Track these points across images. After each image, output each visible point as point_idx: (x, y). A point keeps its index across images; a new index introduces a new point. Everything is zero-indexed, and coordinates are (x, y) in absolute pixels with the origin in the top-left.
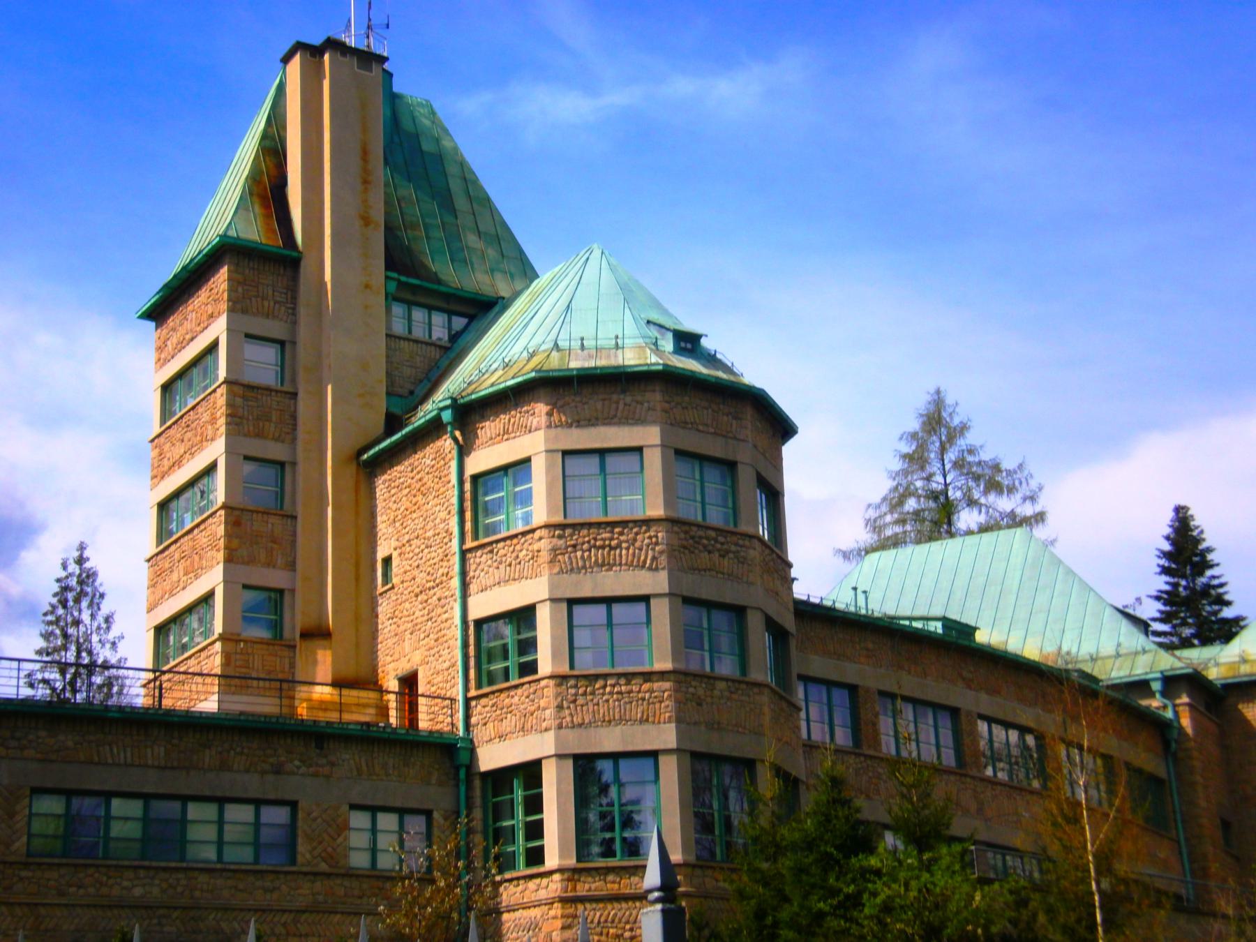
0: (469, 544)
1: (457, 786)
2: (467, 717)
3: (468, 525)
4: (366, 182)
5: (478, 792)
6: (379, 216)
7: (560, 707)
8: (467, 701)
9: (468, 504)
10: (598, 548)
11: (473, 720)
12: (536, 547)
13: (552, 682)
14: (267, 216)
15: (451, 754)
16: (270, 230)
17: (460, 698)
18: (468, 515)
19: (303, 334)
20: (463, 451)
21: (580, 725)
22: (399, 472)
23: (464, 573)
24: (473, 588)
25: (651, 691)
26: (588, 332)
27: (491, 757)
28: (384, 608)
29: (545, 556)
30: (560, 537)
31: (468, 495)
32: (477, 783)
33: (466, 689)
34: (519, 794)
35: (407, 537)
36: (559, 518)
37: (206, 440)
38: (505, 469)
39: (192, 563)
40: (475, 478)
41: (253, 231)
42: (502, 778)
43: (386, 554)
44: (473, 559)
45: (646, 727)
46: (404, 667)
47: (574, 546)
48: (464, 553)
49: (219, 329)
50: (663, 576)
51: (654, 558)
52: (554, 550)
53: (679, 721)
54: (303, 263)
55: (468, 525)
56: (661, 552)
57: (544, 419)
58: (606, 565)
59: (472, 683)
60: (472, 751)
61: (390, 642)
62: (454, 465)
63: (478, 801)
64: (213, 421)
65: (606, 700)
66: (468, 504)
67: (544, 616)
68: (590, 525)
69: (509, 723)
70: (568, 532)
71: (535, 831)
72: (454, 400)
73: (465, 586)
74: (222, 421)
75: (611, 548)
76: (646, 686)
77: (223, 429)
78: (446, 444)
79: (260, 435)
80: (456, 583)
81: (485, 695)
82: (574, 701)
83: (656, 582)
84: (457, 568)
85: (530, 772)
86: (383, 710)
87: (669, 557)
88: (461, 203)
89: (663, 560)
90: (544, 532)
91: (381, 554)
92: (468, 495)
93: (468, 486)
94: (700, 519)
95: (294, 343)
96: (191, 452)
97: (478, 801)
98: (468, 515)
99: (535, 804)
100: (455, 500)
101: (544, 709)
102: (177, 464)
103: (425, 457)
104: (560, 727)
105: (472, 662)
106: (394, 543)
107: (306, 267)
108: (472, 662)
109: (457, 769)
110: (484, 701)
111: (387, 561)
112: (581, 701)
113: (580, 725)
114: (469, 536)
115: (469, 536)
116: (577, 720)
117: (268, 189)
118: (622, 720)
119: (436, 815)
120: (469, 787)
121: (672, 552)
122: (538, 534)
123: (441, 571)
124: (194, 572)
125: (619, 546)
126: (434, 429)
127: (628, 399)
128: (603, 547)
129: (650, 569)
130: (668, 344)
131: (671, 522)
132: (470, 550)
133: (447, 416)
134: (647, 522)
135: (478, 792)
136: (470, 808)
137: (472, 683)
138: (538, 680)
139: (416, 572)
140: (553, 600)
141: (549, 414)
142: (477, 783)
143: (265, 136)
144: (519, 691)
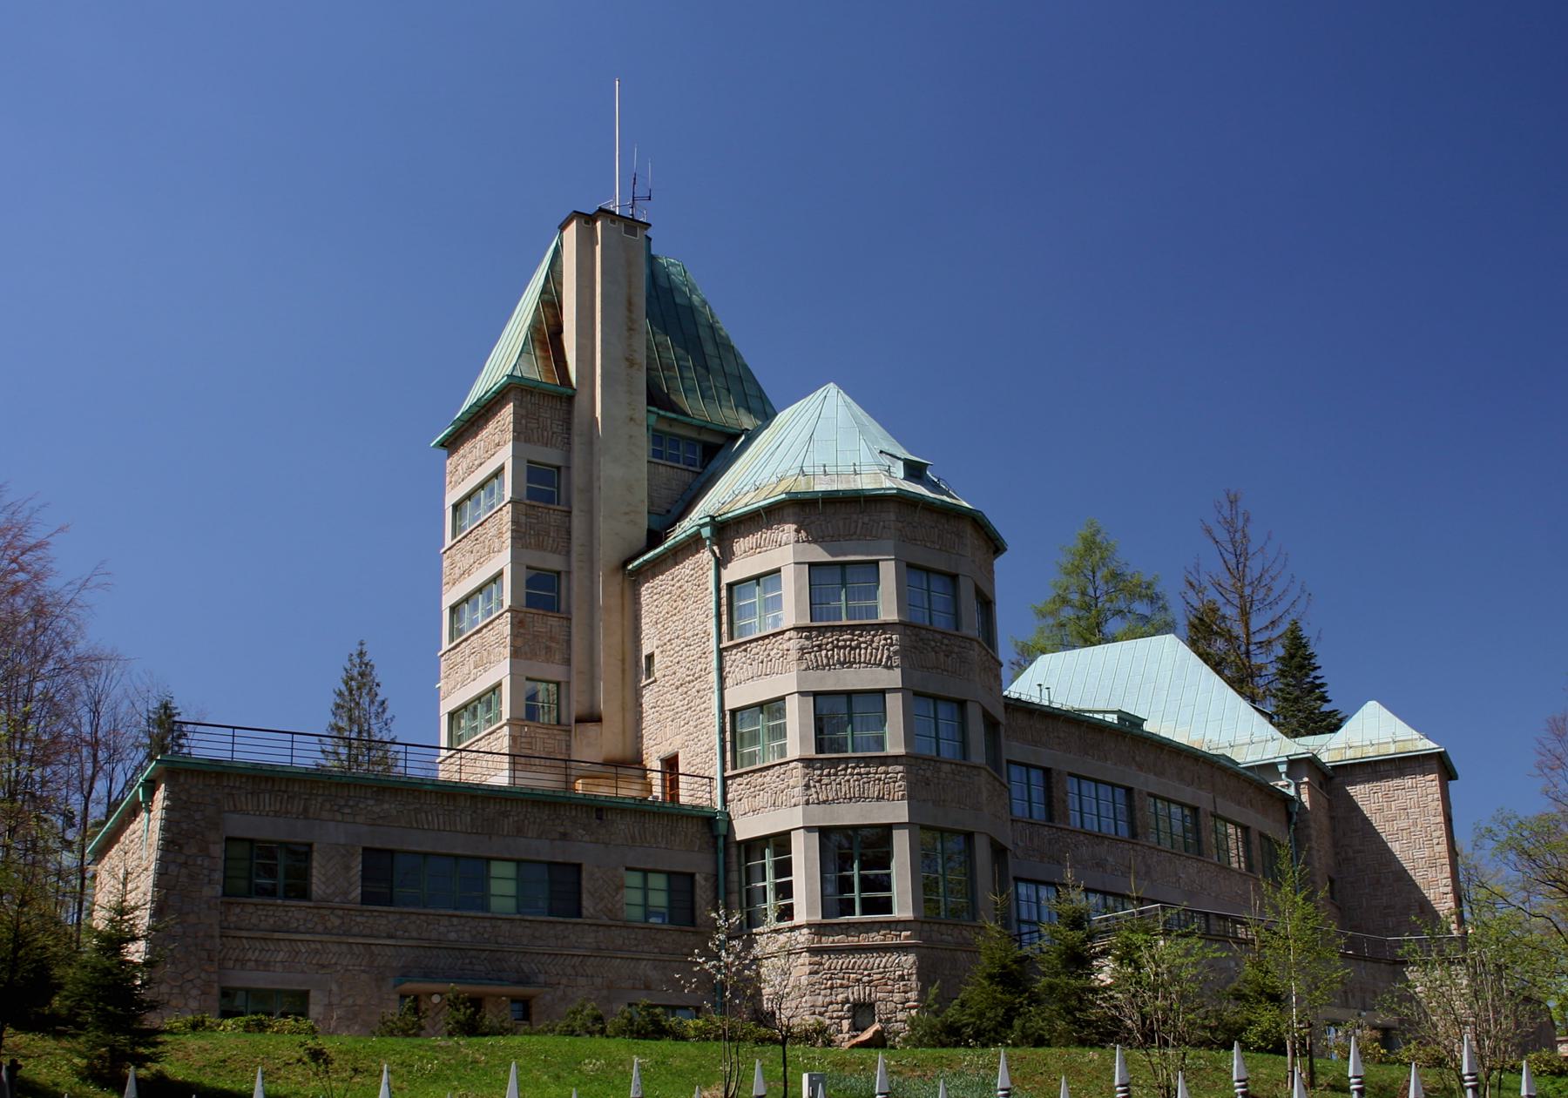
17: (718, 777)
24: (729, 682)
26: (830, 461)
27: (744, 829)
32: (734, 851)
42: (754, 846)
44: (729, 658)
60: (730, 823)
62: (712, 573)
69: (763, 799)
78: (705, 557)
81: (740, 775)
85: (781, 842)
97: (734, 867)
100: (713, 605)
109: (716, 838)
110: (738, 780)
124: (483, 666)
126: (693, 544)
135: (734, 859)
136: (727, 871)
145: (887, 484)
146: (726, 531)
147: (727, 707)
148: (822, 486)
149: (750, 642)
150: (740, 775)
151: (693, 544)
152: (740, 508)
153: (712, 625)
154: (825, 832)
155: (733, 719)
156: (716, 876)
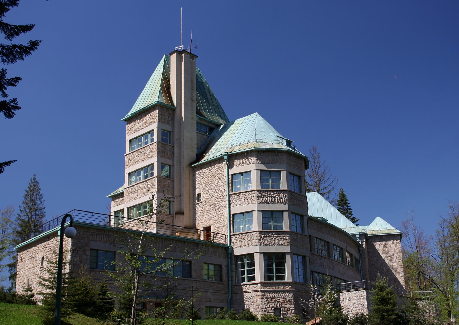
0: (231, 193)
1: (228, 259)
2: (231, 240)
3: (231, 188)
4: (192, 89)
5: (233, 261)
6: (195, 98)
7: (260, 240)
8: (230, 236)
9: (230, 182)
10: (270, 197)
11: (232, 241)
12: (253, 195)
13: (258, 233)
14: (166, 96)
15: (227, 250)
16: (167, 101)
18: (230, 185)
19: (176, 130)
20: (230, 167)
21: (265, 245)
22: (205, 171)
23: (229, 201)
24: (232, 205)
27: (238, 251)
28: (198, 208)
29: (256, 198)
30: (260, 193)
31: (230, 179)
32: (233, 258)
33: (230, 233)
34: (245, 262)
35: (207, 189)
36: (259, 188)
37: (148, 157)
38: (242, 173)
39: (143, 191)
40: (232, 175)
41: (164, 101)
42: (241, 257)
43: (199, 193)
44: (232, 197)
45: (283, 246)
46: (206, 225)
47: (264, 196)
48: (229, 195)
49: (155, 126)
51: (285, 201)
52: (258, 197)
54: (176, 110)
55: (231, 188)
56: (287, 200)
57: (255, 161)
58: (272, 202)
59: (232, 231)
60: (232, 249)
61: (200, 217)
62: (226, 171)
63: (234, 263)
64: (152, 152)
65: (272, 239)
66: (230, 182)
68: (268, 191)
69: (244, 243)
70: (262, 192)
71: (253, 271)
72: (228, 153)
73: (230, 204)
74: (156, 152)
75: (274, 198)
78: (224, 164)
79: (165, 157)
80: (227, 203)
81: (236, 235)
82: (264, 238)
83: (285, 207)
84: (227, 199)
86: (199, 236)
87: (289, 201)
88: (209, 97)
89: (287, 202)
90: (255, 192)
91: (198, 192)
92: (230, 179)
93: (230, 177)
94: (293, 190)
95: (173, 132)
96: (143, 160)
97: (234, 263)
98: (230, 185)
99: (252, 265)
100: (227, 180)
101: (256, 240)
102: (137, 162)
103: (215, 168)
104: (260, 245)
105: (232, 225)
106: (202, 190)
107: (177, 111)
108: (232, 225)
109: (228, 254)
110: (235, 236)
111: (199, 195)
112: (266, 238)
113: (265, 245)
114: (231, 191)
115: (231, 191)
116: (265, 243)
117: (165, 88)
118: (276, 244)
119: (223, 266)
120: (231, 259)
121: (288, 200)
122: (253, 192)
123: (220, 199)
127: (278, 158)
128: (271, 197)
129: (284, 204)
130: (285, 143)
131: (288, 192)
132: (231, 195)
133: (225, 157)
134: (283, 191)
135: (233, 261)
137: (232, 231)
140: (258, 211)
141: (257, 160)
142: (233, 258)
143: (163, 74)
144: (247, 234)
145: (283, 147)
146: (231, 158)
147: (232, 213)
148: (263, 146)
149: (240, 193)
150: (236, 235)
151: (219, 160)
152: (237, 150)
153: (226, 187)
154: (265, 254)
155: (233, 217)
156: (228, 266)
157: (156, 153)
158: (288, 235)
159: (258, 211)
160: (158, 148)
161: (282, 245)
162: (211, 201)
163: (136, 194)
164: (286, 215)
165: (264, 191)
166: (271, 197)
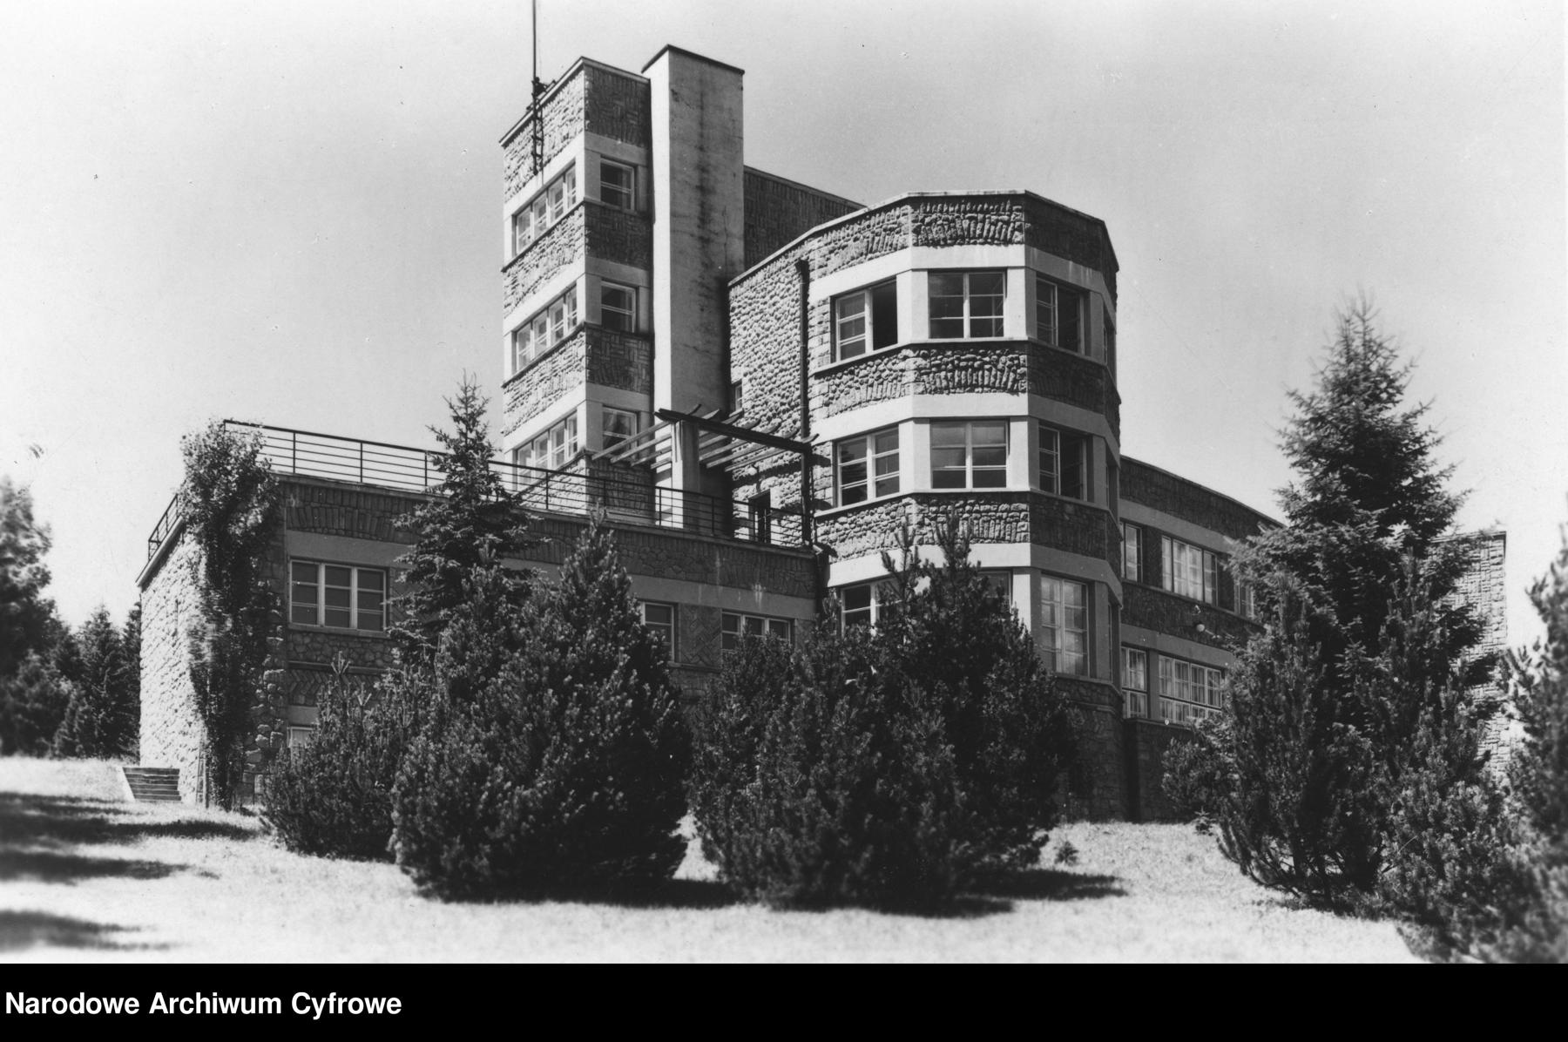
10: (961, 369)
12: (901, 365)
25: (1008, 511)
29: (910, 376)
30: (925, 357)
35: (759, 362)
47: (938, 366)
50: (1024, 398)
51: (1015, 381)
52: (918, 369)
53: (1033, 541)
58: (971, 387)
67: (907, 433)
74: (582, 241)
75: (975, 370)
76: (1004, 506)
77: (582, 250)
82: (935, 519)
83: (1018, 404)
90: (909, 352)
91: (734, 379)
102: (532, 289)
106: (744, 370)
125: (981, 368)
128: (965, 368)
134: (1012, 346)
138: (899, 499)
139: (768, 397)
157: (581, 243)
158: (1024, 506)
159: (918, 420)
160: (588, 225)
161: (1000, 540)
162: (771, 404)
163: (532, 399)
164: (1020, 434)
165: (942, 348)
166: (965, 368)
